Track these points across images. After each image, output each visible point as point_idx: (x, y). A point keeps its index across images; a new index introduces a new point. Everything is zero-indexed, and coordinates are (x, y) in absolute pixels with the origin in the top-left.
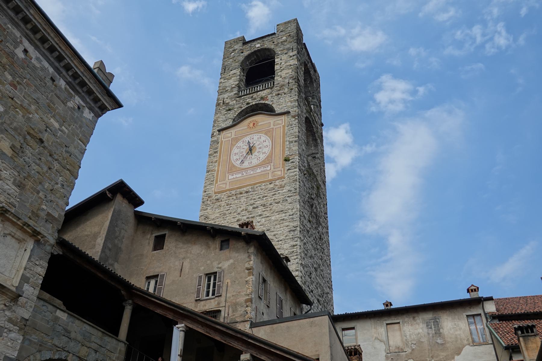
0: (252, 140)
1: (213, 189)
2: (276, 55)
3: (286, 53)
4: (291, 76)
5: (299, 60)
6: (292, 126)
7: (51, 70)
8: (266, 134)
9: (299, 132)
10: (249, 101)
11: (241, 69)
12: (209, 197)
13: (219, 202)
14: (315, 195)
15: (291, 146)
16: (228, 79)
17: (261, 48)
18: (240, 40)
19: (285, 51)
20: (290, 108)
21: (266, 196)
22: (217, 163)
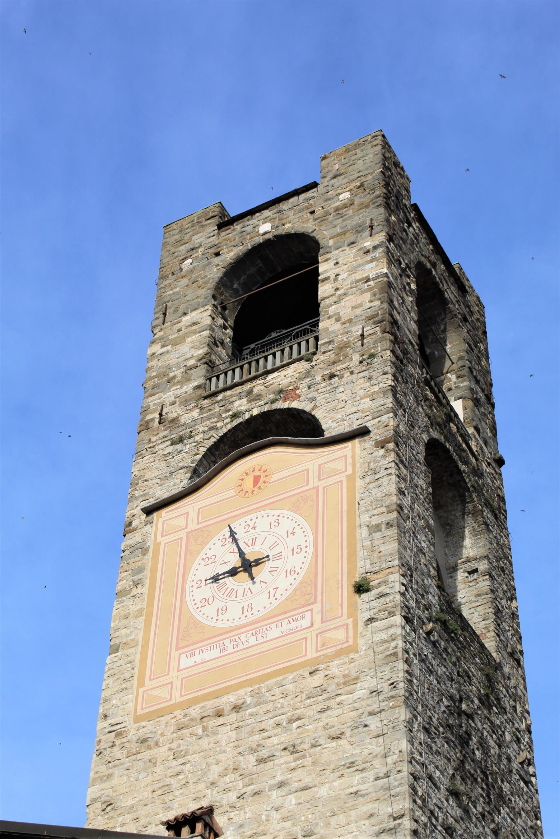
0: (252, 531)
1: (131, 705)
2: (321, 251)
3: (353, 243)
4: (369, 313)
5: (392, 260)
6: (378, 476)
8: (295, 508)
9: (401, 492)
10: (240, 406)
11: (214, 305)
12: (119, 735)
13: (149, 748)
14: (476, 701)
15: (376, 543)
16: (175, 343)
17: (276, 233)
18: (211, 215)
19: (350, 237)
20: (369, 417)
21: (299, 719)
22: (142, 619)
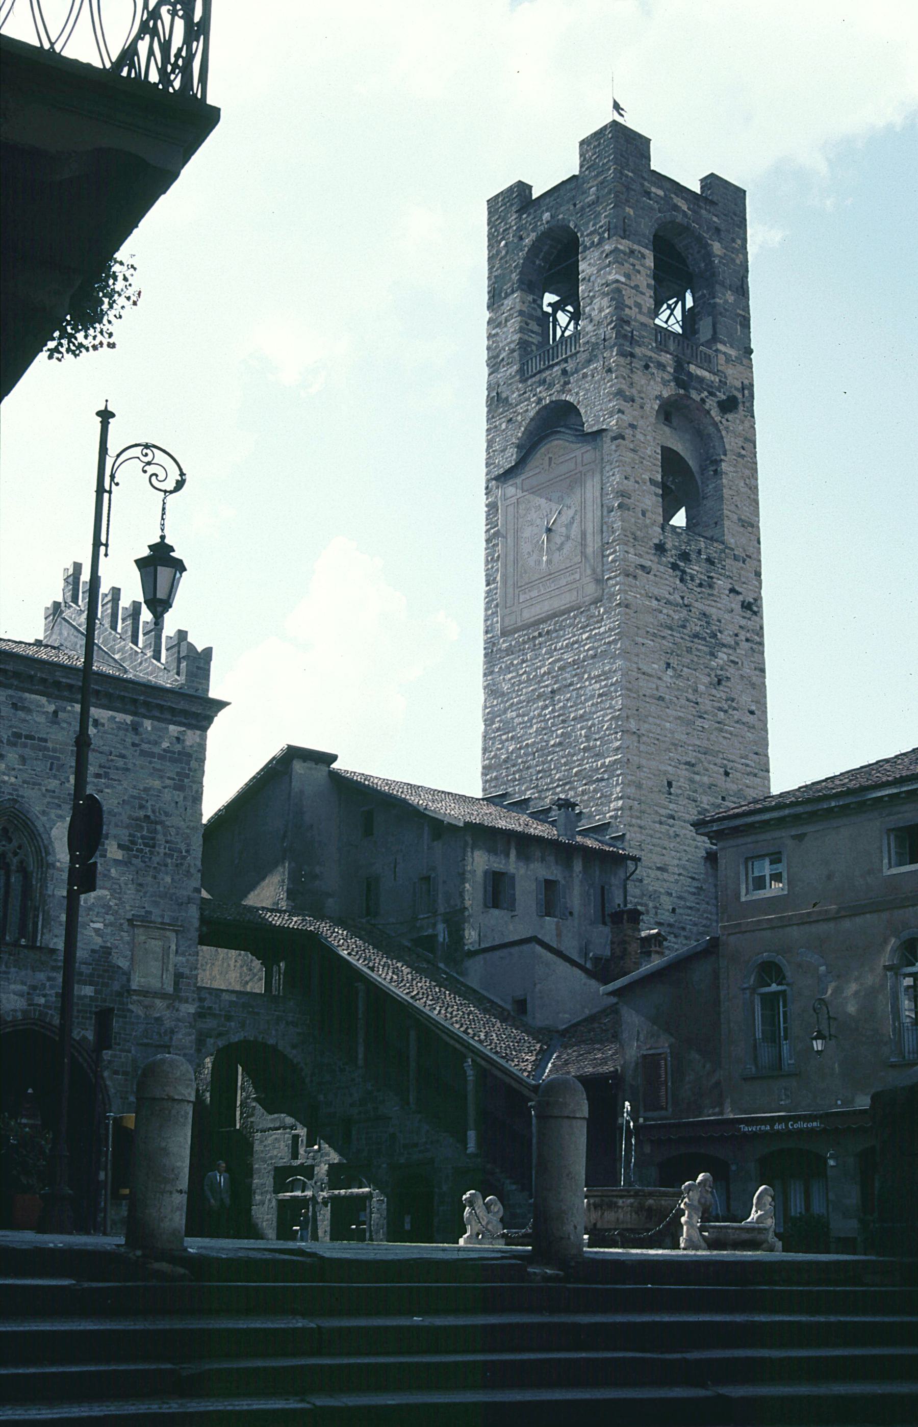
7: (129, 719)
10: (540, 392)
12: (494, 644)
